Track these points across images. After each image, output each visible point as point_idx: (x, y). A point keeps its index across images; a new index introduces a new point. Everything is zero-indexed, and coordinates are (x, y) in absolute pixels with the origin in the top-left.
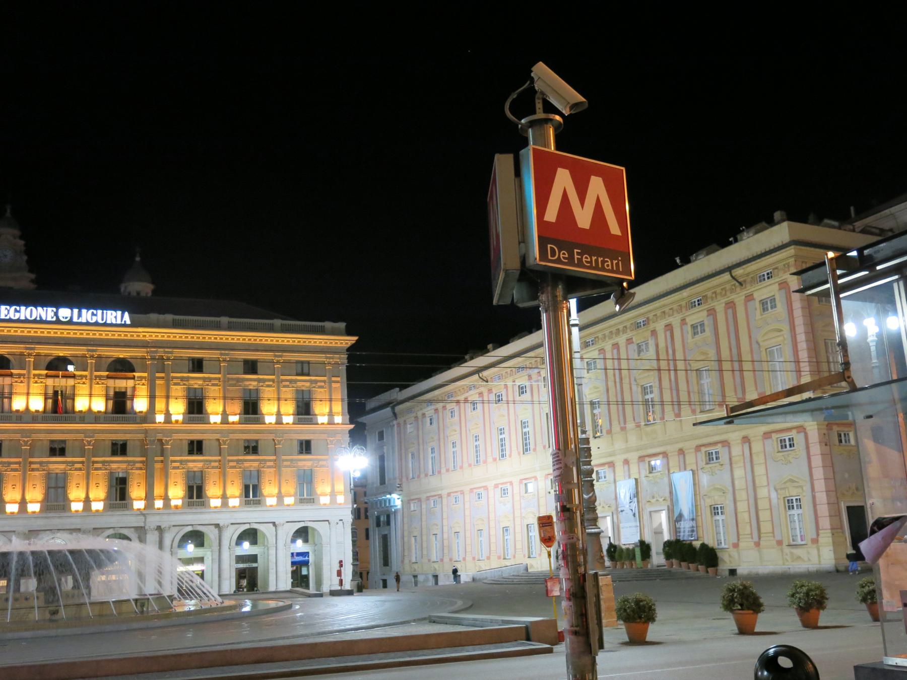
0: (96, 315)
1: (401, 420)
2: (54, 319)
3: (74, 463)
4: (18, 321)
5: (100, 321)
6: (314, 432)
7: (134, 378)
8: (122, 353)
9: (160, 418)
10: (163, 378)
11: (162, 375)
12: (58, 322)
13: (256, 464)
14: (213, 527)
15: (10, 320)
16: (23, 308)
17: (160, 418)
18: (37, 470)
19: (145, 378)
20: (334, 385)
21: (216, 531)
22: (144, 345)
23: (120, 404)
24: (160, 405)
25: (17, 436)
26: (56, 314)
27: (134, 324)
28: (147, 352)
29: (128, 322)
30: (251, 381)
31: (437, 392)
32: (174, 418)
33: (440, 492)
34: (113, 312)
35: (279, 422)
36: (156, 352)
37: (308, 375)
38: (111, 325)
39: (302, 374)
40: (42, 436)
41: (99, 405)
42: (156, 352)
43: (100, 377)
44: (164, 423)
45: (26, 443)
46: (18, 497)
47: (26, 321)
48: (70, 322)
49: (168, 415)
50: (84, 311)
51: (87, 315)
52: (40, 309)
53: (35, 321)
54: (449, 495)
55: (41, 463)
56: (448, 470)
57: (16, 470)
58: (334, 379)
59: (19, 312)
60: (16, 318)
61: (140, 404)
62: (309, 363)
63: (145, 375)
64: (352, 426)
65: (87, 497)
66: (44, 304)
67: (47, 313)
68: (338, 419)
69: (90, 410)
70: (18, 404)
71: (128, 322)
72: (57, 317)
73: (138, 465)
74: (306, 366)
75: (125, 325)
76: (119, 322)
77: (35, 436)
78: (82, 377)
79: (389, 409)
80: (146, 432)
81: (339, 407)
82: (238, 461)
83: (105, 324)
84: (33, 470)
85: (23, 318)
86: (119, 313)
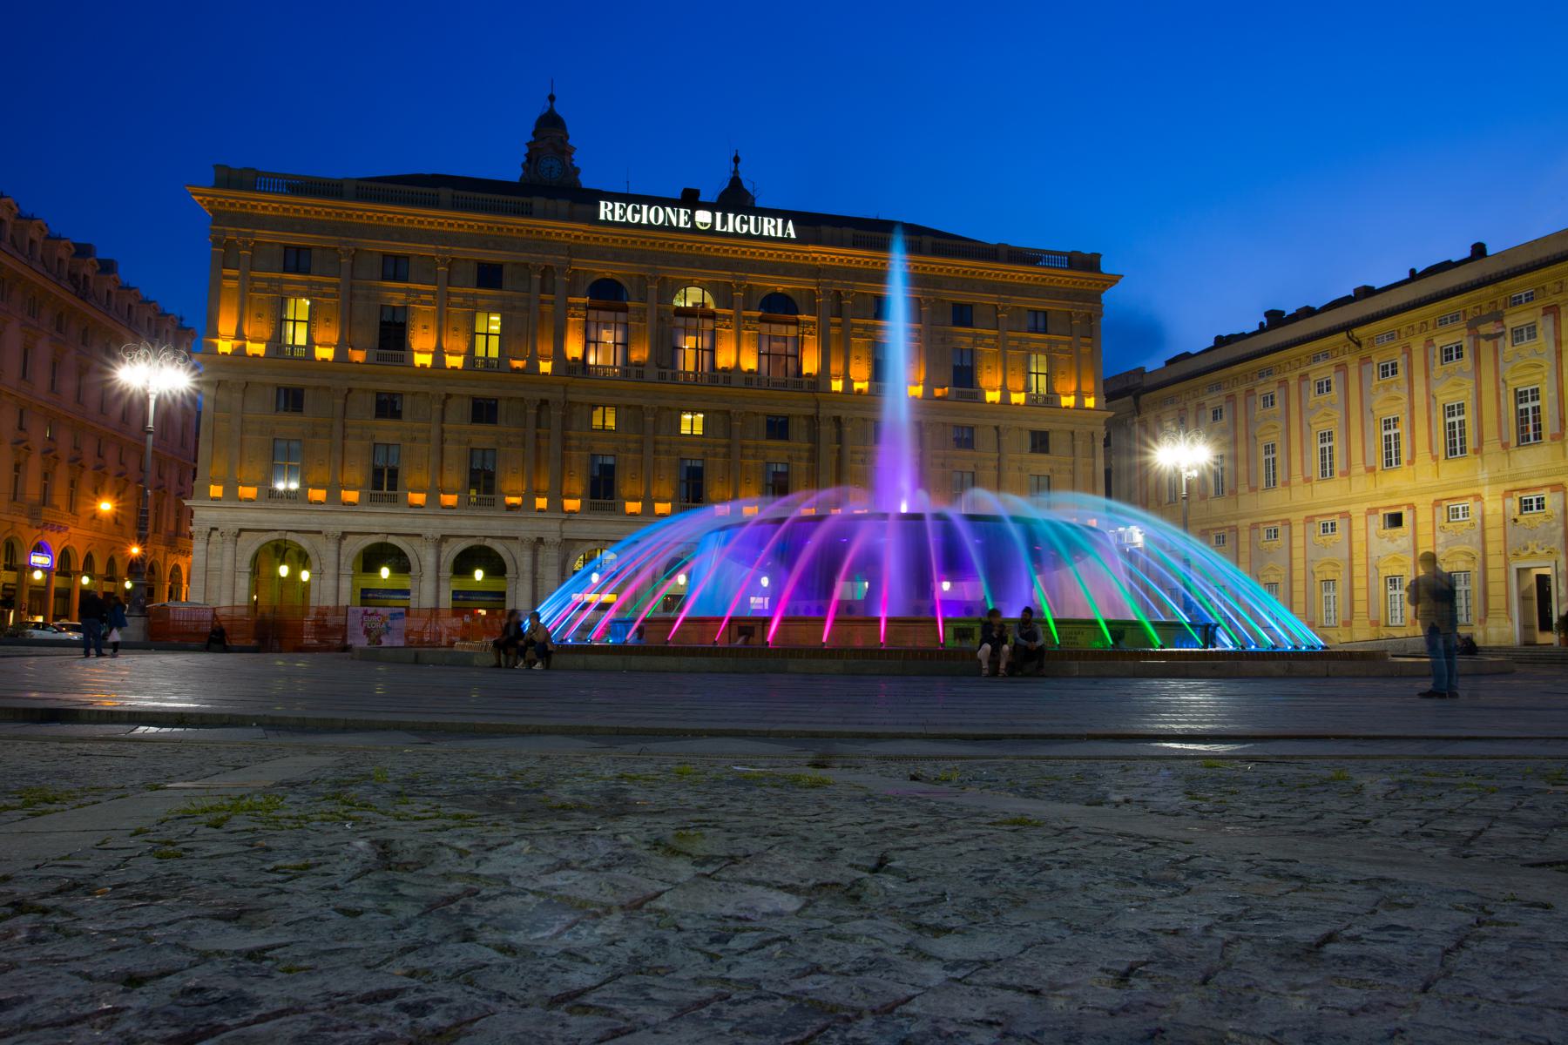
1: (1150, 416)
4: (639, 225)
7: (797, 323)
8: (781, 286)
12: (694, 230)
15: (627, 225)
16: (645, 207)
17: (837, 386)
19: (813, 323)
22: (816, 272)
23: (783, 360)
24: (836, 367)
26: (692, 218)
29: (793, 236)
30: (964, 337)
31: (1237, 368)
33: (1233, 523)
36: (831, 284)
37: (1045, 332)
38: (769, 238)
39: (1036, 331)
41: (750, 363)
42: (831, 284)
43: (750, 319)
47: (650, 226)
48: (712, 231)
49: (848, 382)
51: (734, 223)
52: (668, 210)
53: (661, 228)
54: (1254, 526)
56: (1253, 489)
59: (640, 212)
61: (810, 364)
63: (813, 319)
64: (1111, 414)
66: (675, 204)
67: (680, 218)
71: (793, 236)
72: (694, 223)
74: (1041, 316)
75: (788, 240)
78: (725, 317)
81: (1088, 385)
83: (761, 237)
85: (645, 221)
86: (780, 221)
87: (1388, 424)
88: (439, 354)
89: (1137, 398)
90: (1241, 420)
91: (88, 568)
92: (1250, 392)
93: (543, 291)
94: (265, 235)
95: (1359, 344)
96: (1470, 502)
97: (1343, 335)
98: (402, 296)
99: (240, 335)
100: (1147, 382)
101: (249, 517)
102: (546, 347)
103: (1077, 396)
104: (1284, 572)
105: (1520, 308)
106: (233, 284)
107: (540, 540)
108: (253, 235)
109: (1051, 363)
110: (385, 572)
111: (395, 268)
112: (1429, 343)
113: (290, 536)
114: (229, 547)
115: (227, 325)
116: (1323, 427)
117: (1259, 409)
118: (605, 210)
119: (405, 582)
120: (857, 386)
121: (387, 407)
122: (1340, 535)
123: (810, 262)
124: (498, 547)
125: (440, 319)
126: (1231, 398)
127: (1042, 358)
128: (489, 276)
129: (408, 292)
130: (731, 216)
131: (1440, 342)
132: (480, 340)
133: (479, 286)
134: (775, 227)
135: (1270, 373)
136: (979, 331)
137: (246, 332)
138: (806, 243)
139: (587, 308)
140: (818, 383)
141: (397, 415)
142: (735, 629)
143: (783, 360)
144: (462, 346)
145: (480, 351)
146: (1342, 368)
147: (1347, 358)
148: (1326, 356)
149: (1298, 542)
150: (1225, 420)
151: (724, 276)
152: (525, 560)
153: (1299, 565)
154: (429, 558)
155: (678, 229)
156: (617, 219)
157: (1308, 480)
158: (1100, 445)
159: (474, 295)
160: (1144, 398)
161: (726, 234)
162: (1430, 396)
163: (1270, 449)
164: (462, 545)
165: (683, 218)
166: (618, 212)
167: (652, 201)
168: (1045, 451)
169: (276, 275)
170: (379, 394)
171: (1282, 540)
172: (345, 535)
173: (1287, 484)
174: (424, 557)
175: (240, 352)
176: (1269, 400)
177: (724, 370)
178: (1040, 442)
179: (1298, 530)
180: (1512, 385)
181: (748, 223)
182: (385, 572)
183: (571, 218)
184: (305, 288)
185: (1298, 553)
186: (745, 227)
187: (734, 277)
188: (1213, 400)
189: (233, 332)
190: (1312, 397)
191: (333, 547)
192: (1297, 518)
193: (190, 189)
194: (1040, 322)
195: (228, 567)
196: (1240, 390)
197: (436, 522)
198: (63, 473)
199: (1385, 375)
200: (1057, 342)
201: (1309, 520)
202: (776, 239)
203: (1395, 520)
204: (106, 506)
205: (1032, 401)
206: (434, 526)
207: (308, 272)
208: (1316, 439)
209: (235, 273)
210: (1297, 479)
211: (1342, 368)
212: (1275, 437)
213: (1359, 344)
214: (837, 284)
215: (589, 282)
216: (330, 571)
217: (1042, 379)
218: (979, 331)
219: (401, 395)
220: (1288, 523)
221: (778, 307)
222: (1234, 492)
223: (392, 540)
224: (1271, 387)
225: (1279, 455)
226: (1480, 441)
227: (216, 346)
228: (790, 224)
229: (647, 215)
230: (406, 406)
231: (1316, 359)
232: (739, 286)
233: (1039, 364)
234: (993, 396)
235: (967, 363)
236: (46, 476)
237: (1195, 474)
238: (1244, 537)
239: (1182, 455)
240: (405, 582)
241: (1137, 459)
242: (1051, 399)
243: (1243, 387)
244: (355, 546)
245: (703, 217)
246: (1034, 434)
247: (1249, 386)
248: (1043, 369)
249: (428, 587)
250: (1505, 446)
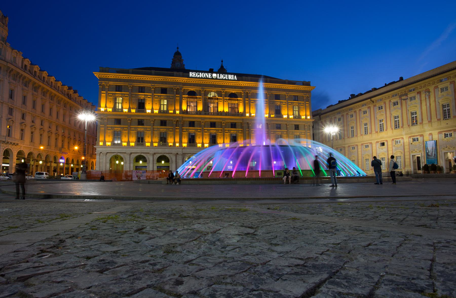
1: (323, 120)
3: (219, 130)
4: (199, 78)
6: (300, 122)
7: (238, 100)
8: (233, 91)
12: (212, 78)
13: (280, 133)
15: (196, 78)
17: (247, 115)
18: (207, 132)
20: (307, 105)
23: (234, 109)
24: (247, 110)
25: (200, 120)
26: (212, 75)
27: (238, 80)
30: (278, 102)
31: (344, 108)
32: (252, 115)
35: (288, 117)
38: (230, 80)
39: (295, 100)
40: (208, 120)
41: (226, 110)
43: (226, 99)
45: (203, 122)
46: (201, 142)
47: (202, 78)
48: (216, 79)
49: (250, 114)
51: (222, 76)
53: (204, 78)
55: (208, 130)
56: (349, 137)
57: (199, 132)
61: (241, 110)
62: (297, 96)
63: (241, 99)
65: (224, 142)
66: (207, 72)
67: (209, 76)
68: (309, 117)
69: (224, 111)
73: (240, 132)
75: (235, 80)
77: (206, 120)
78: (220, 99)
79: (318, 116)
80: (243, 120)
81: (308, 113)
82: (274, 131)
83: (228, 80)
84: (205, 132)
87: (380, 121)
88: (152, 110)
89: (320, 116)
90: (345, 121)
91: (73, 162)
92: (347, 114)
93: (177, 94)
94: (111, 83)
95: (373, 102)
96: (401, 139)
97: (369, 100)
98: (143, 96)
99: (106, 107)
100: (322, 112)
101: (109, 150)
102: (178, 107)
103: (306, 115)
104: (356, 157)
105: (411, 92)
106: (104, 95)
107: (177, 154)
108: (108, 83)
109: (299, 108)
110: (141, 162)
111: (142, 90)
112: (390, 101)
113: (118, 154)
114: (105, 157)
115: (103, 104)
116: (365, 122)
117: (349, 119)
118: (191, 74)
119: (146, 164)
120: (252, 115)
121: (141, 123)
122: (370, 148)
123: (240, 85)
124: (167, 155)
125: (152, 101)
126: (343, 116)
127: (297, 107)
128: (164, 91)
129: (145, 95)
131: (392, 101)
132: (162, 106)
133: (162, 93)
135: (352, 109)
137: (107, 106)
138: (239, 81)
139: (187, 98)
140: (244, 114)
141: (143, 124)
142: (224, 174)
143: (234, 109)
144: (158, 108)
145: (162, 109)
146: (369, 108)
147: (370, 105)
148: (365, 105)
149: (360, 150)
150: (341, 121)
151: (220, 89)
152: (174, 158)
153: (360, 155)
154: (151, 158)
155: (208, 78)
157: (362, 135)
158: (311, 128)
159: (161, 96)
160: (322, 116)
161: (220, 79)
162: (391, 114)
163: (352, 128)
164: (159, 155)
165: (210, 76)
166: (194, 75)
167: (202, 72)
168: (298, 129)
169: (114, 92)
170: (138, 120)
171: (356, 150)
172: (131, 153)
173: (357, 136)
174: (150, 158)
175: (106, 111)
176: (352, 116)
177: (220, 112)
178: (297, 127)
179: (359, 147)
180: (410, 111)
182: (141, 162)
183: (183, 76)
184: (121, 95)
185: (360, 153)
188: (338, 116)
189: (104, 106)
190: (362, 115)
191: (128, 156)
192: (359, 144)
193: (94, 73)
194: (296, 98)
195: (104, 162)
196: (345, 114)
197: (153, 150)
198: (66, 140)
199: (380, 109)
200: (300, 103)
201: (362, 144)
203: (383, 144)
204: (76, 148)
205: (295, 117)
206: (152, 151)
207: (121, 91)
208: (363, 125)
209: (105, 92)
210: (359, 135)
211: (369, 108)
212: (354, 125)
213: (373, 102)
215: (188, 92)
216: (128, 162)
217: (297, 112)
219: (144, 120)
220: (357, 145)
221: (233, 96)
222: (344, 138)
223: (142, 154)
224: (352, 112)
225: (355, 129)
226: (403, 125)
227: (100, 110)
229: (201, 75)
230: (145, 122)
231: (363, 106)
233: (296, 109)
234: (285, 117)
235: (279, 109)
236: (62, 141)
237: (334, 134)
238: (347, 149)
239: (331, 130)
240: (146, 164)
241: (320, 131)
242: (299, 117)
243: (346, 113)
244: (134, 156)
245: (214, 75)
246: (295, 125)
247: (347, 112)
248: (297, 110)
249: (151, 166)
250: (409, 126)
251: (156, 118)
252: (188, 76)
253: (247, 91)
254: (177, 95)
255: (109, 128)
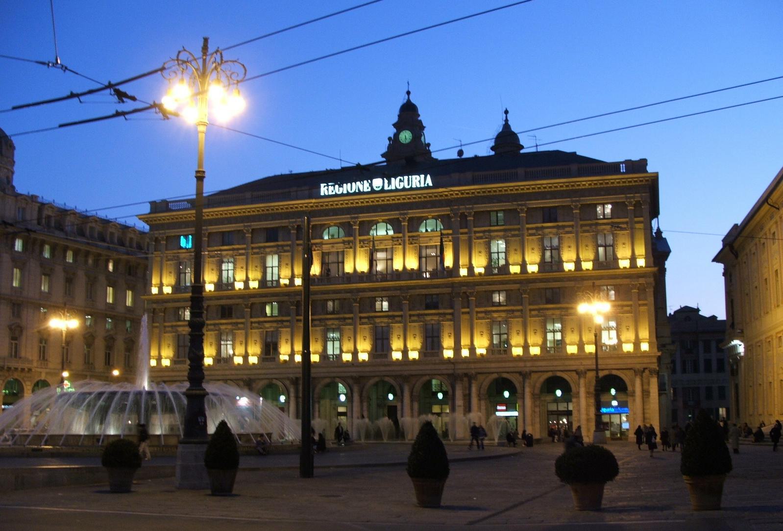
0: (403, 181)
2: (369, 190)
4: (342, 195)
5: (407, 187)
9: (463, 272)
10: (466, 233)
11: (466, 230)
12: (373, 191)
14: (518, 375)
15: (336, 195)
17: (463, 272)
20: (638, 226)
21: (521, 379)
24: (463, 260)
26: (371, 185)
28: (451, 210)
29: (431, 184)
34: (417, 176)
38: (417, 189)
41: (412, 263)
42: (458, 209)
44: (468, 276)
47: (348, 194)
48: (383, 191)
50: (393, 179)
52: (358, 183)
53: (355, 194)
58: (636, 219)
60: (340, 193)
61: (449, 262)
68: (641, 262)
70: (348, 268)
71: (431, 184)
72: (372, 188)
75: (428, 187)
76: (422, 185)
83: (411, 189)
85: (345, 192)
86: (422, 176)
102: (298, 270)
128: (272, 235)
130: (393, 179)
132: (269, 270)
134: (420, 182)
136: (560, 224)
144: (259, 275)
145: (269, 278)
155: (364, 193)
156: (330, 193)
159: (265, 247)
181: (403, 181)
186: (402, 184)
187: (401, 214)
202: (421, 188)
214: (462, 209)
218: (560, 224)
228: (429, 176)
232: (404, 219)
251: (253, 300)
252: (319, 196)
253: (462, 209)
254: (298, 242)
255: (168, 329)
